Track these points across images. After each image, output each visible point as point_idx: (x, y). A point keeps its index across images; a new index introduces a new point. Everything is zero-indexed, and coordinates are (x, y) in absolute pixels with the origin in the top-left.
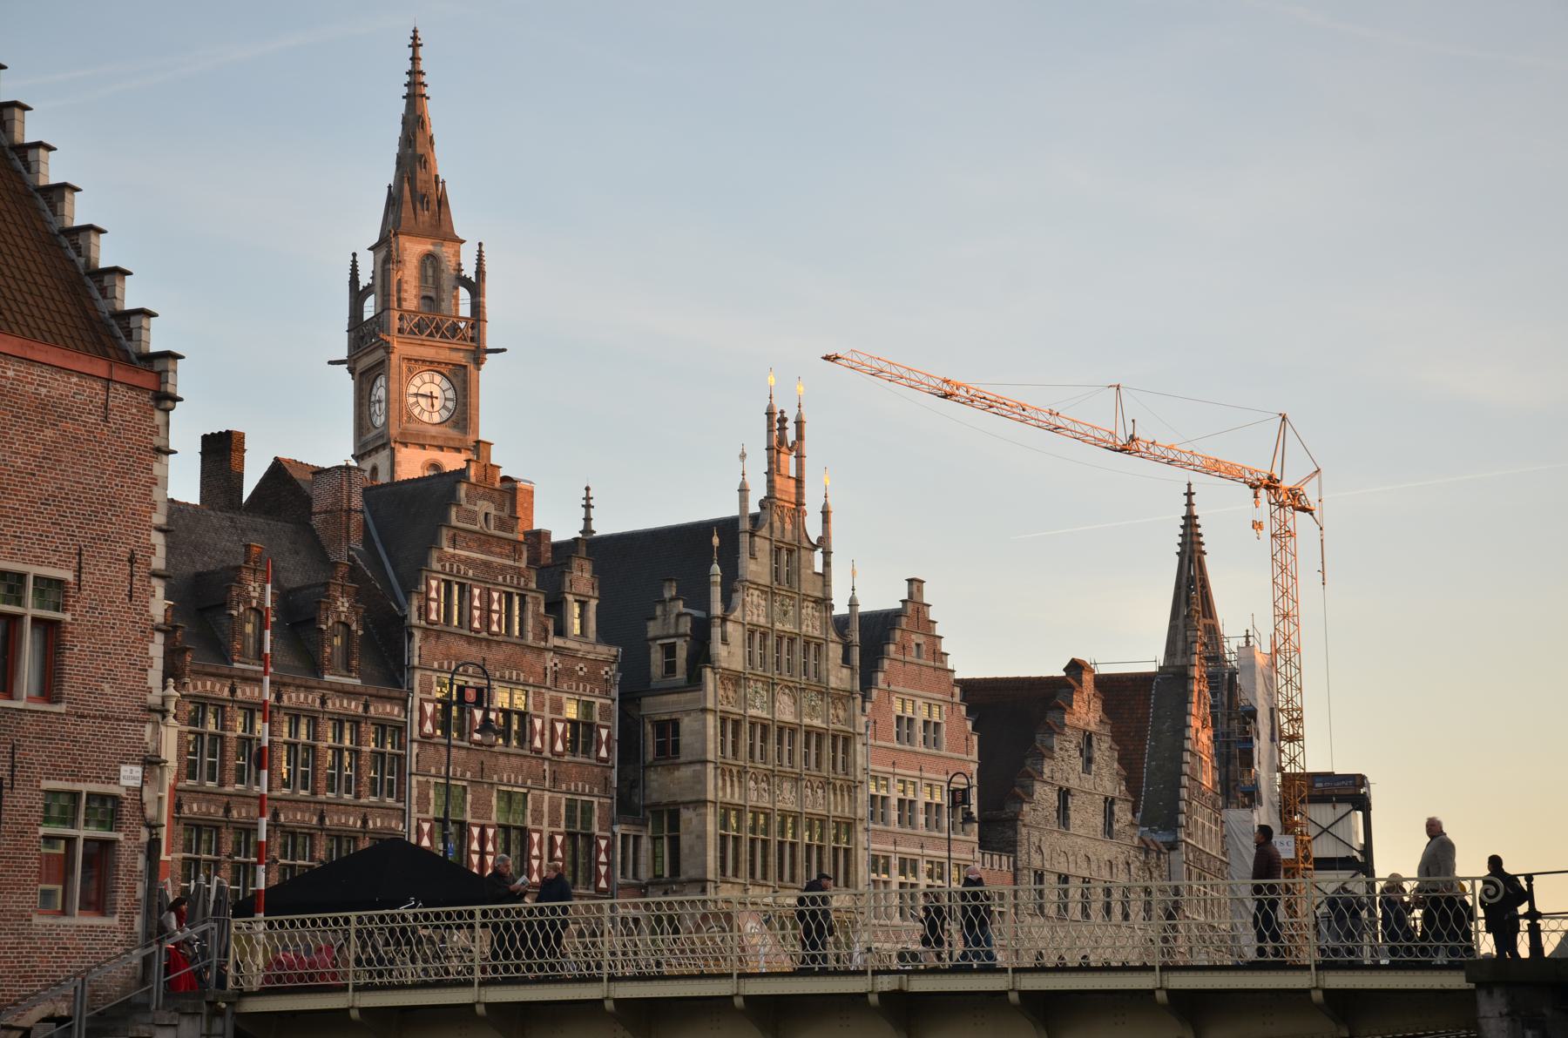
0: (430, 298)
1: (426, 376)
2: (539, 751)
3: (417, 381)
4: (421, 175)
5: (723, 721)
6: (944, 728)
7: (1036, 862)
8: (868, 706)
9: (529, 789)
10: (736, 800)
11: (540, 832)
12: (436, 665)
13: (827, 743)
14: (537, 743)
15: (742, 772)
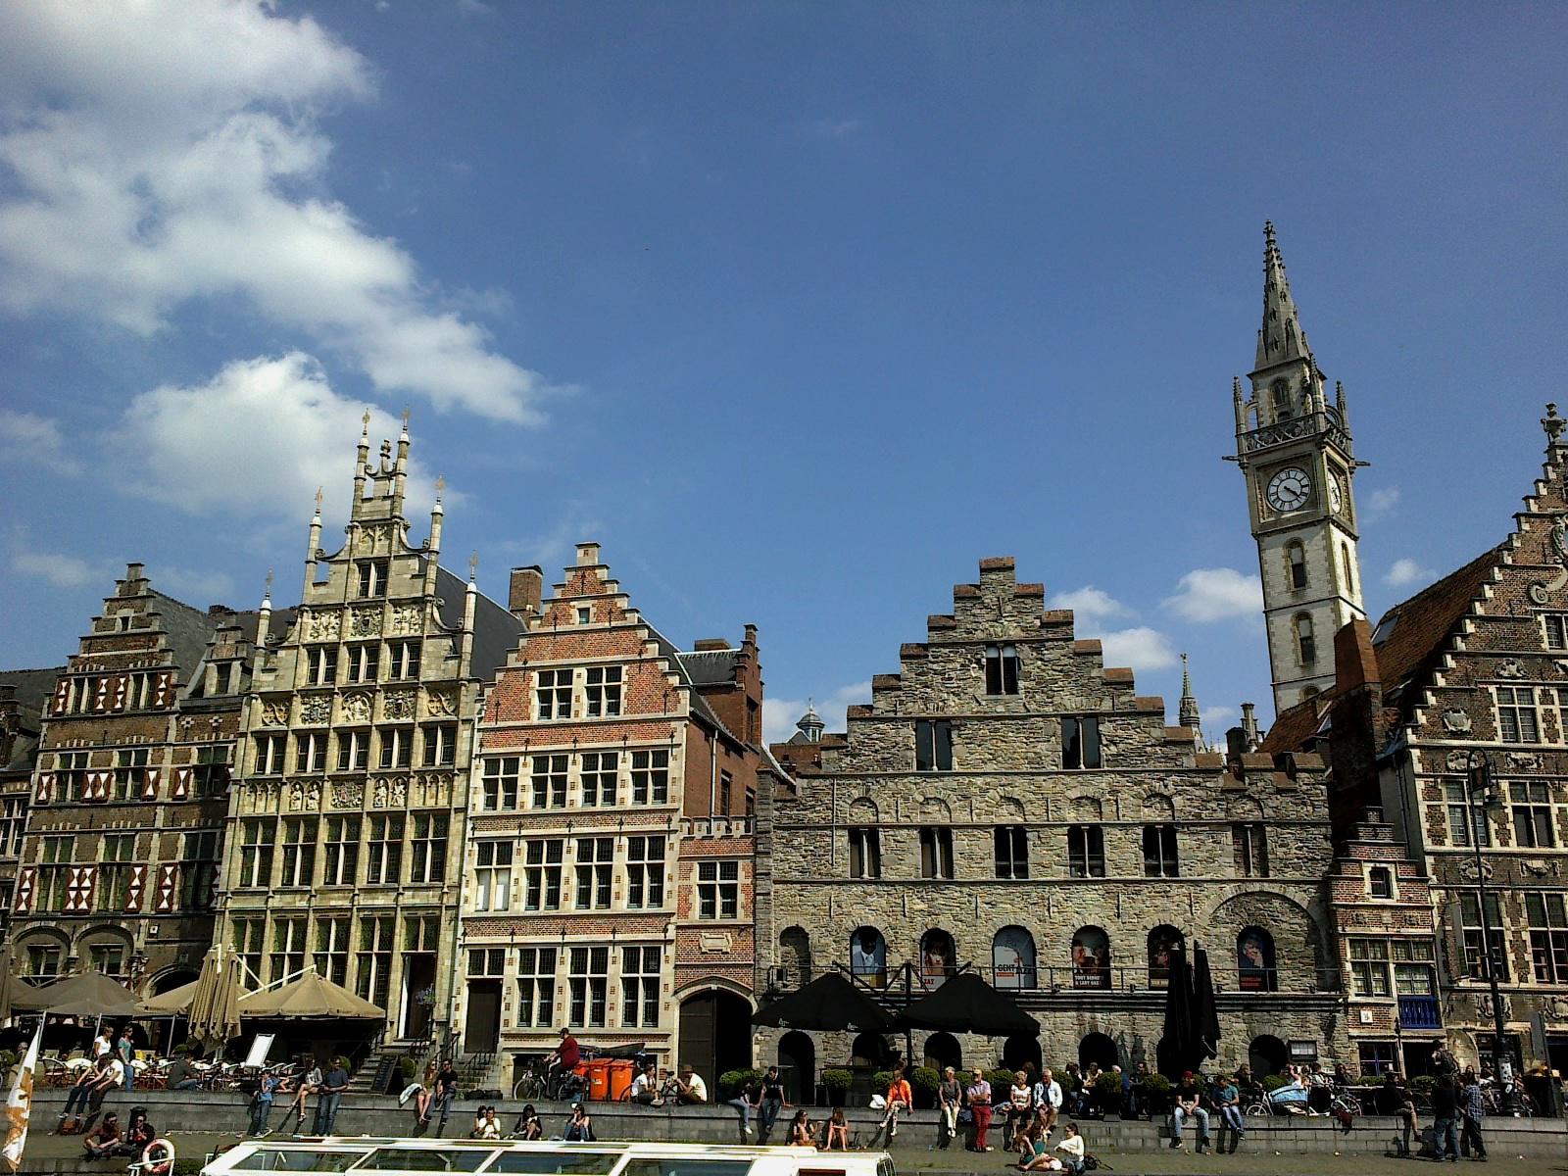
0: (1286, 413)
1: (1283, 476)
2: (153, 798)
3: (1276, 482)
4: (1272, 324)
5: (261, 738)
6: (624, 689)
7: (863, 816)
8: (488, 691)
9: (138, 831)
10: (272, 810)
11: (144, 866)
12: (59, 745)
13: (419, 736)
14: (150, 792)
15: (277, 785)
